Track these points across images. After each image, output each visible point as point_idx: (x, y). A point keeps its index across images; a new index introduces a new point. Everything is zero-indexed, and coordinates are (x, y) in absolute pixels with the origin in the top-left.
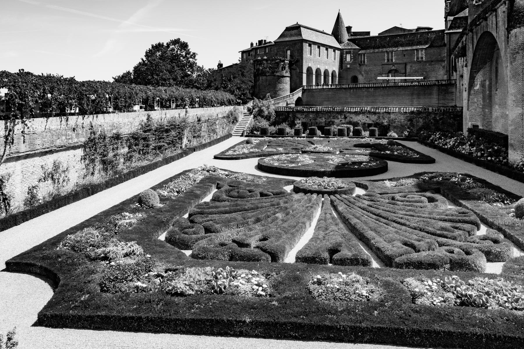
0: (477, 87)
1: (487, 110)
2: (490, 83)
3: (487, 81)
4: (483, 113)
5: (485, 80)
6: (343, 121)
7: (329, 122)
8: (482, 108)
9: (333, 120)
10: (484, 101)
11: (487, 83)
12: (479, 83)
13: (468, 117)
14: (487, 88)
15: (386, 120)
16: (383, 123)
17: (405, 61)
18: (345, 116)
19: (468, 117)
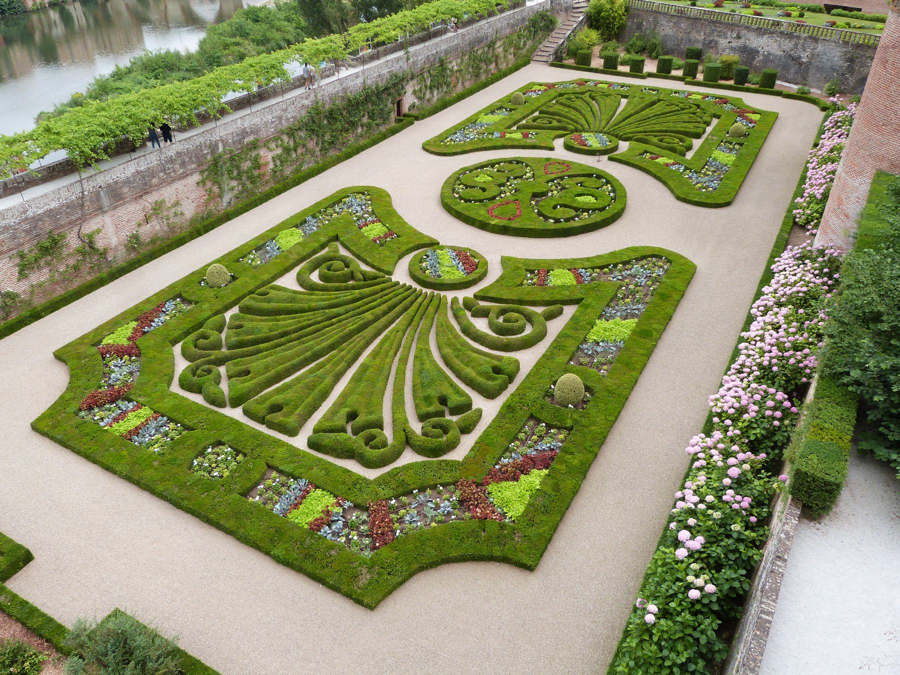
6: (734, 44)
7: (711, 42)
9: (716, 38)
15: (809, 52)
16: (800, 57)
18: (739, 33)
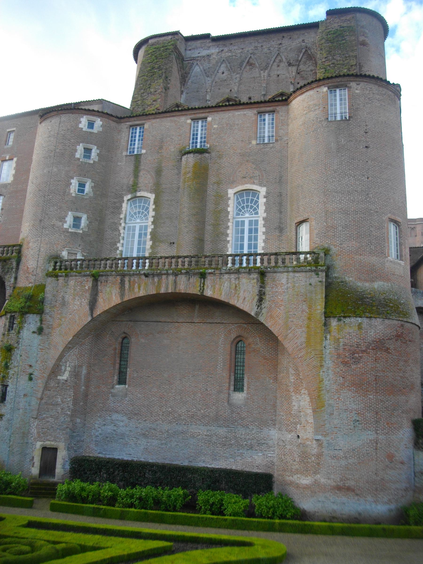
0: (65, 376)
1: (78, 420)
2: (88, 373)
3: (84, 368)
4: (71, 426)
5: (80, 366)
8: (72, 416)
10: (75, 404)
11: (84, 371)
12: (68, 369)
13: (34, 431)
14: (83, 380)
19: (34, 431)
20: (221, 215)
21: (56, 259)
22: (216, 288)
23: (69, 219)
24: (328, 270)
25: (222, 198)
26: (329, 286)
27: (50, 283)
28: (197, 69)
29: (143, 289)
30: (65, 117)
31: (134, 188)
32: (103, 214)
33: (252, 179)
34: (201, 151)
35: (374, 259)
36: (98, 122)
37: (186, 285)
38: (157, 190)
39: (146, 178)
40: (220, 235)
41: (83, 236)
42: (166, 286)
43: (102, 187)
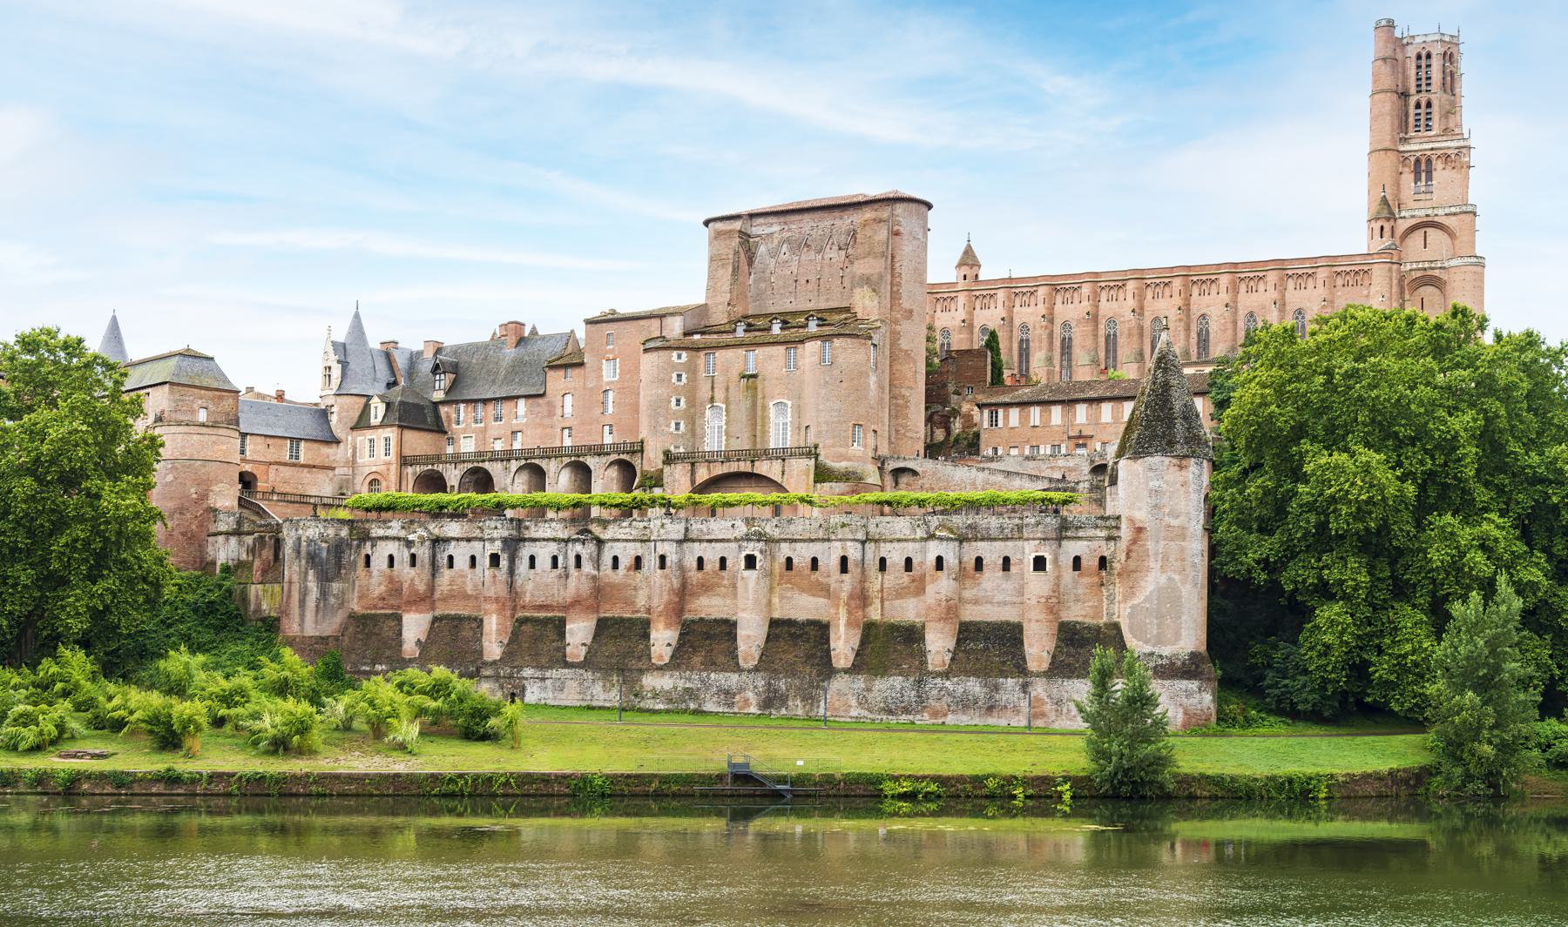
17: (270, 458)
20: (765, 418)
21: (667, 453)
22: (763, 468)
23: (673, 425)
24: (817, 456)
25: (764, 408)
26: (816, 467)
27: (667, 469)
28: (762, 249)
29: (719, 470)
30: (661, 353)
31: (712, 400)
32: (693, 419)
33: (781, 394)
34: (754, 376)
35: (842, 450)
36: (684, 354)
37: (744, 467)
38: (727, 401)
39: (719, 394)
40: (765, 432)
41: (682, 436)
42: (733, 467)
43: (692, 402)
